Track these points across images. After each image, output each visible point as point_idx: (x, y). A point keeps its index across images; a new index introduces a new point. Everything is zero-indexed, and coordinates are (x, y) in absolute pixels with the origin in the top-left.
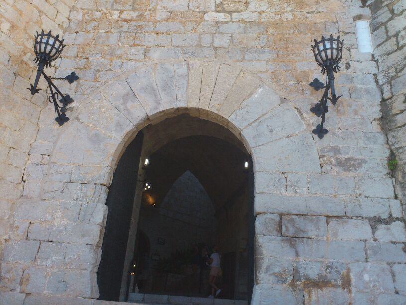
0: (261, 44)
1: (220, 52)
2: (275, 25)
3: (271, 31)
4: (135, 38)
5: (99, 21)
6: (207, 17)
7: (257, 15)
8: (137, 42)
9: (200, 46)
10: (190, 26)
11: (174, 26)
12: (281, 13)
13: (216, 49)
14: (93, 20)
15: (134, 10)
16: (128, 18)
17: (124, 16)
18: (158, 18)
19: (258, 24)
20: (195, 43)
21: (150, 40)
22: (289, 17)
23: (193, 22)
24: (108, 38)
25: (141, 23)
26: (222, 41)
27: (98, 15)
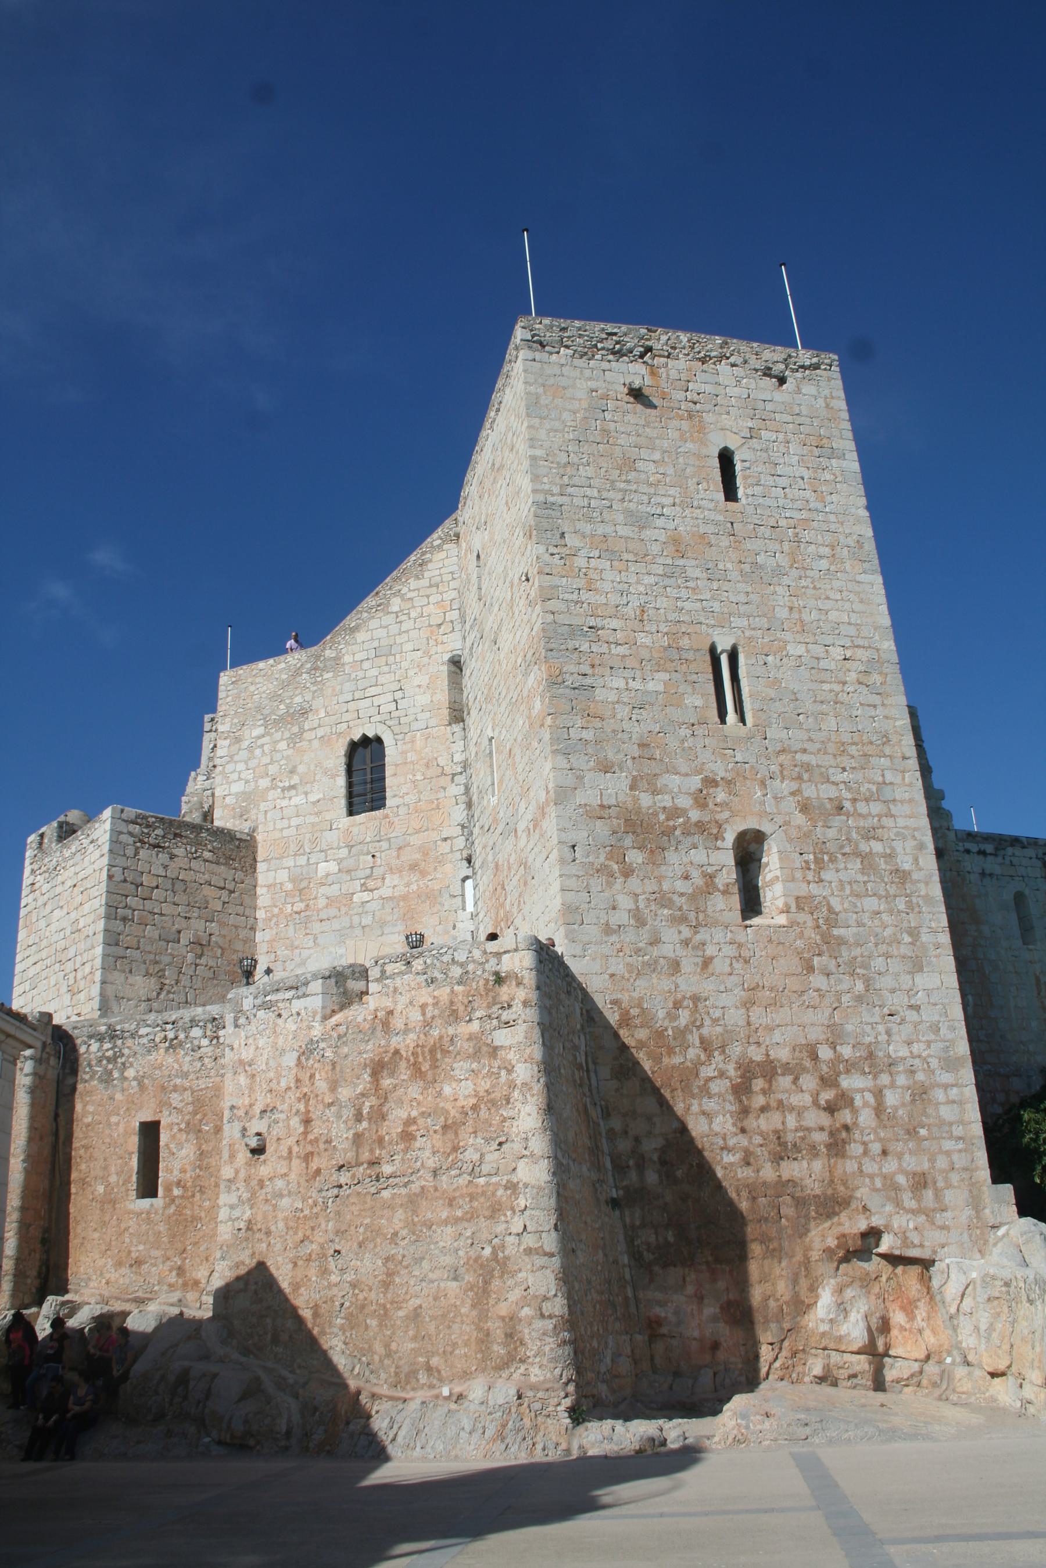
0: (395, 917)
1: (367, 929)
2: (404, 898)
3: (402, 904)
4: (306, 928)
5: (277, 916)
6: (356, 898)
7: (391, 890)
8: (308, 931)
9: (351, 927)
10: (344, 910)
11: (333, 911)
12: (408, 885)
13: (363, 927)
14: (274, 916)
15: (302, 901)
16: (299, 910)
17: (295, 909)
18: (320, 907)
19: (391, 898)
20: (348, 925)
21: (316, 927)
22: (414, 887)
23: (345, 905)
24: (287, 931)
25: (308, 913)
26: (367, 920)
27: (276, 911)
